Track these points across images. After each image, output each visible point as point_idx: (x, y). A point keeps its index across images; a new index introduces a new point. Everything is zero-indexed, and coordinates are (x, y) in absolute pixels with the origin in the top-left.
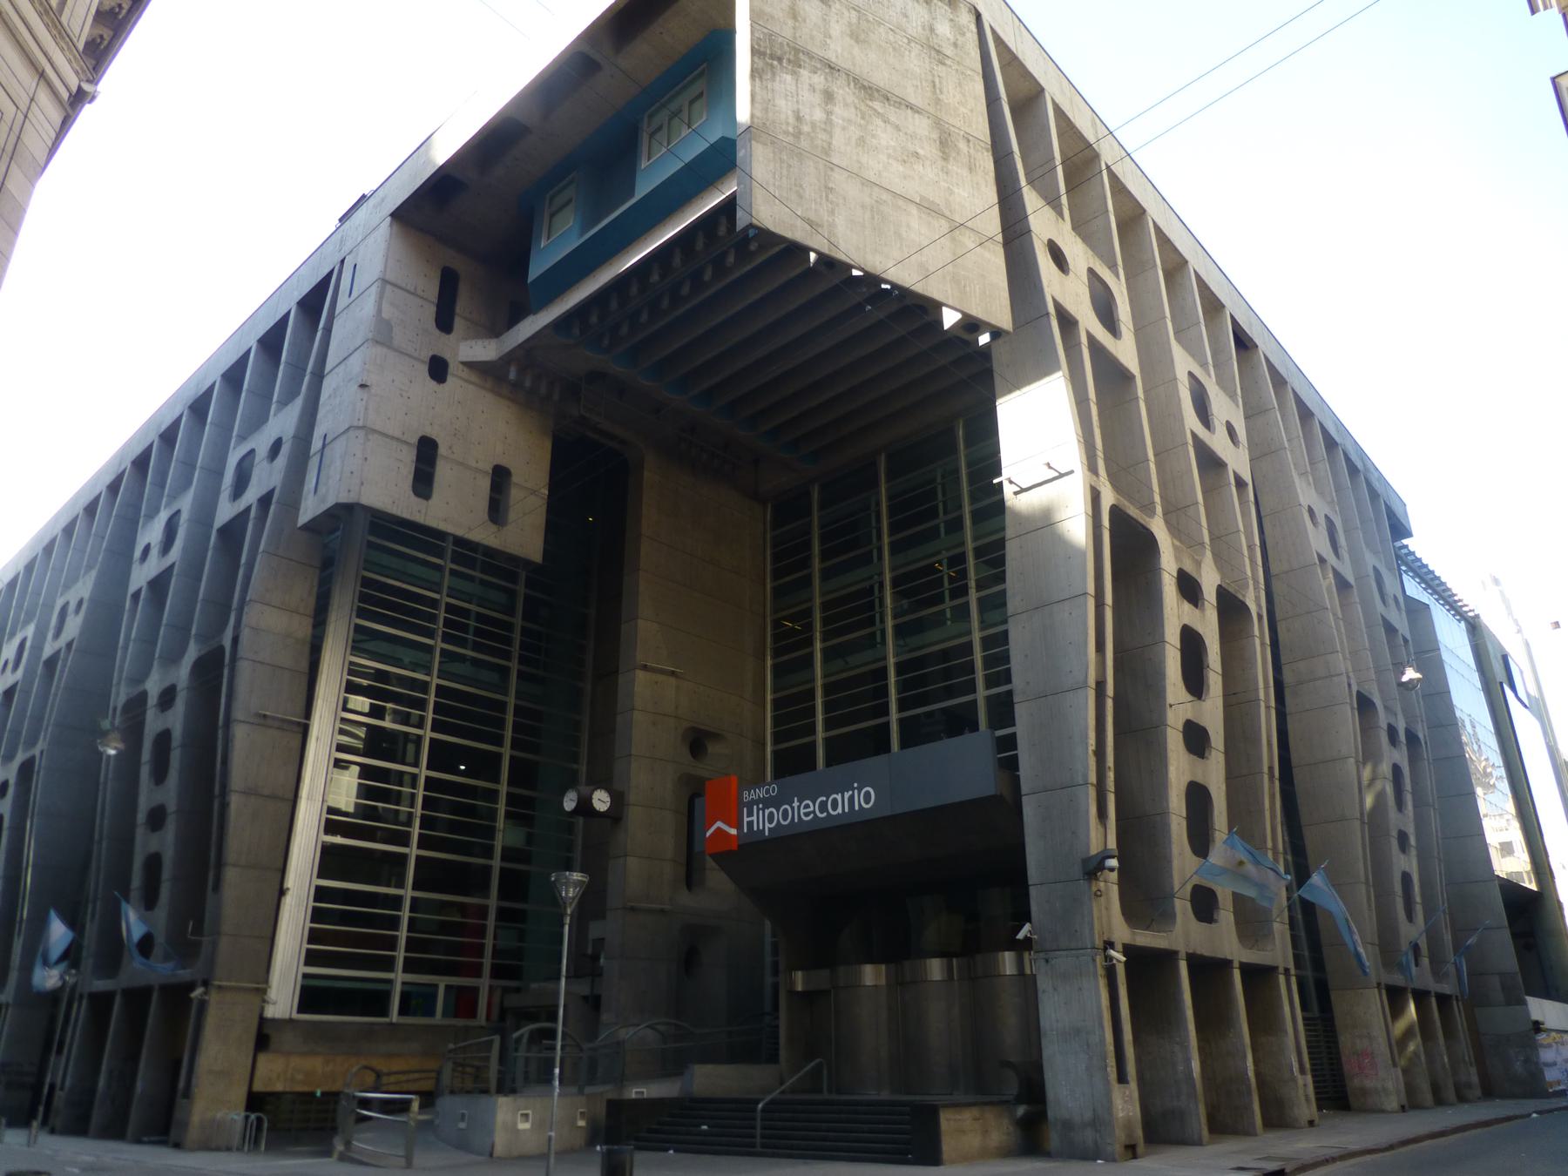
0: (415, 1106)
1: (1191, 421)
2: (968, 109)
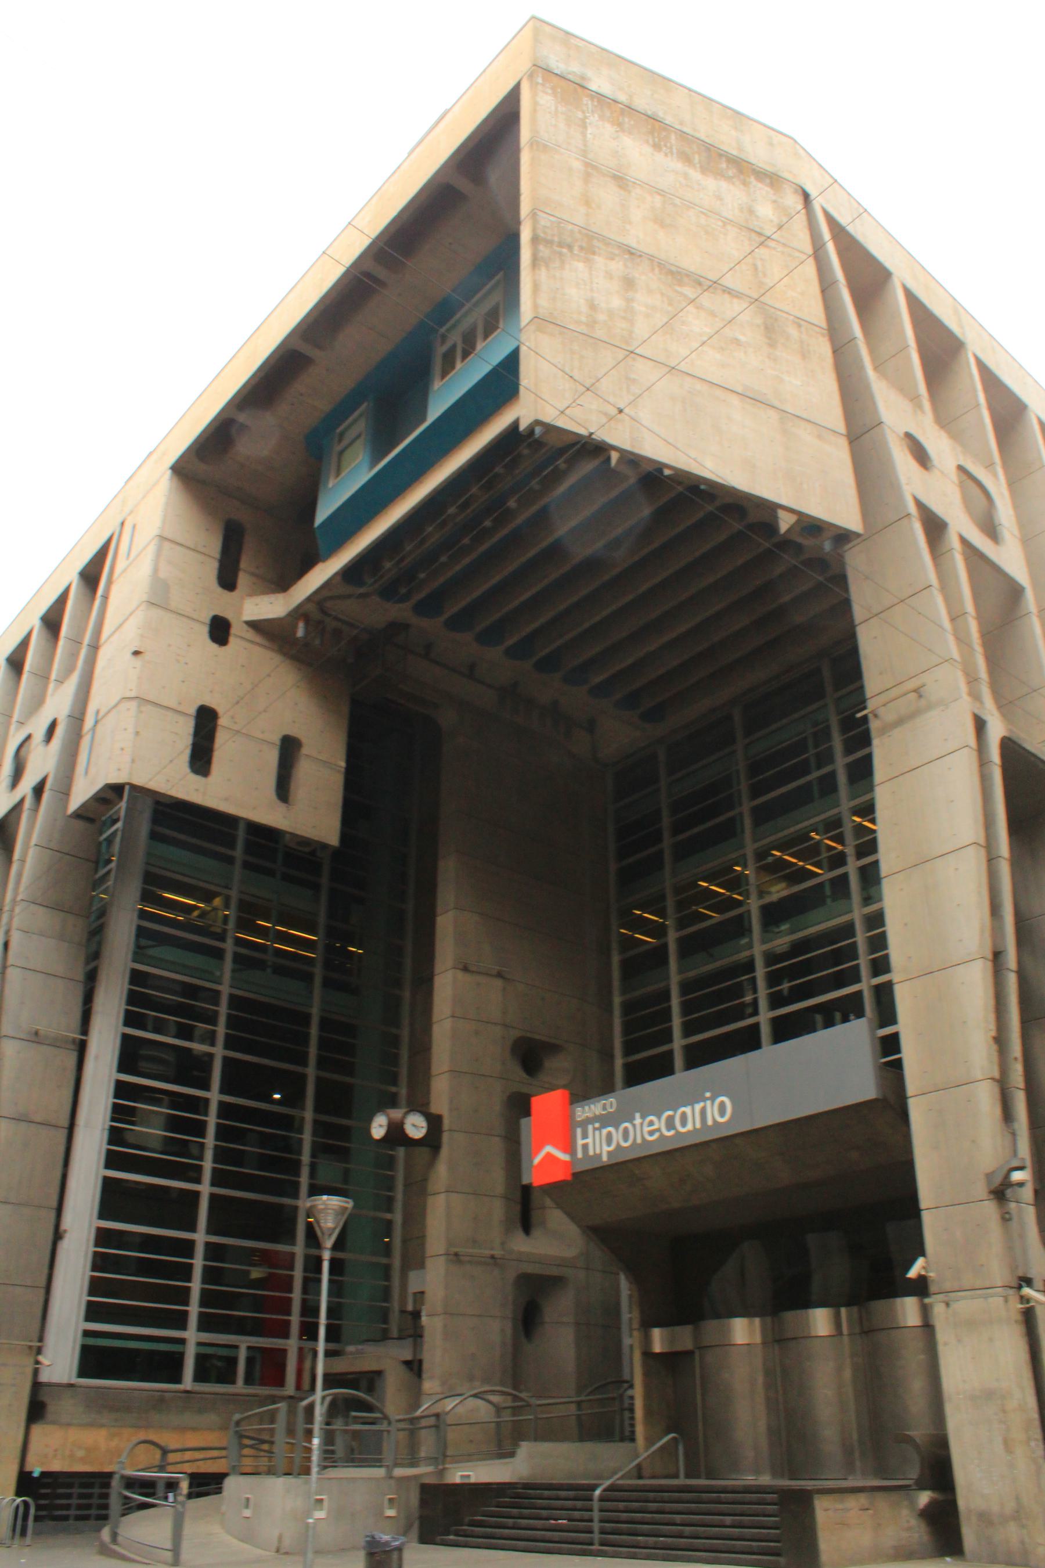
2: (799, 293)
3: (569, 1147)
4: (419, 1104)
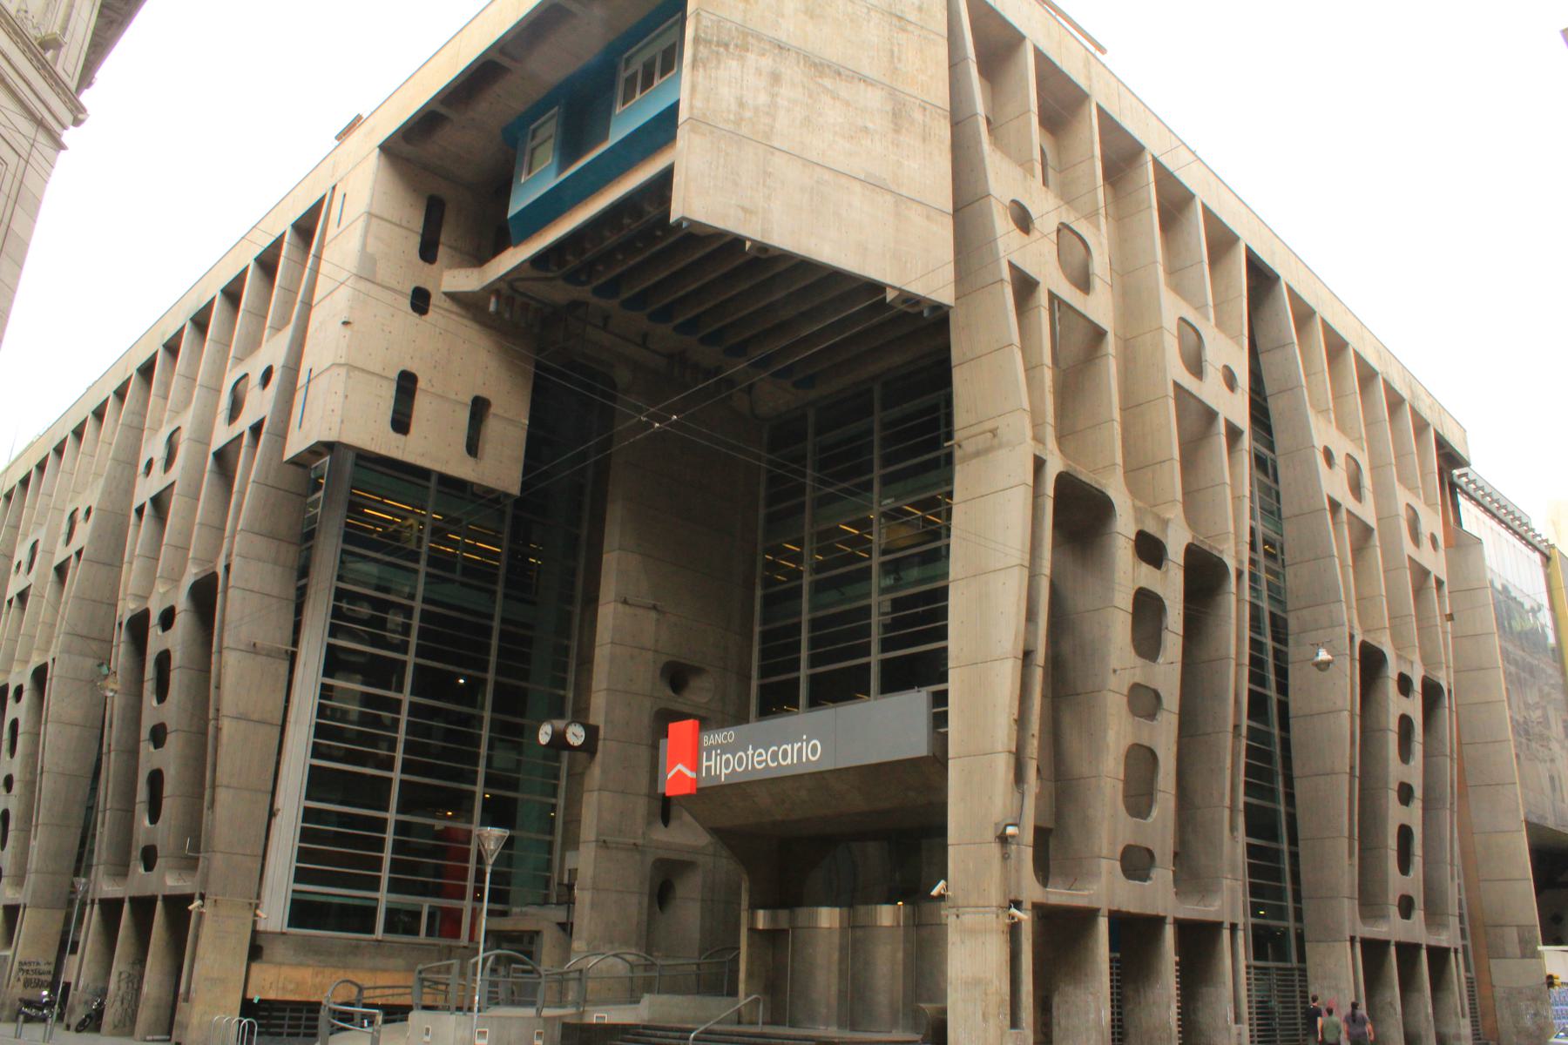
0: (380, 1018)
1: (1177, 371)
3: (696, 766)
4: (580, 716)
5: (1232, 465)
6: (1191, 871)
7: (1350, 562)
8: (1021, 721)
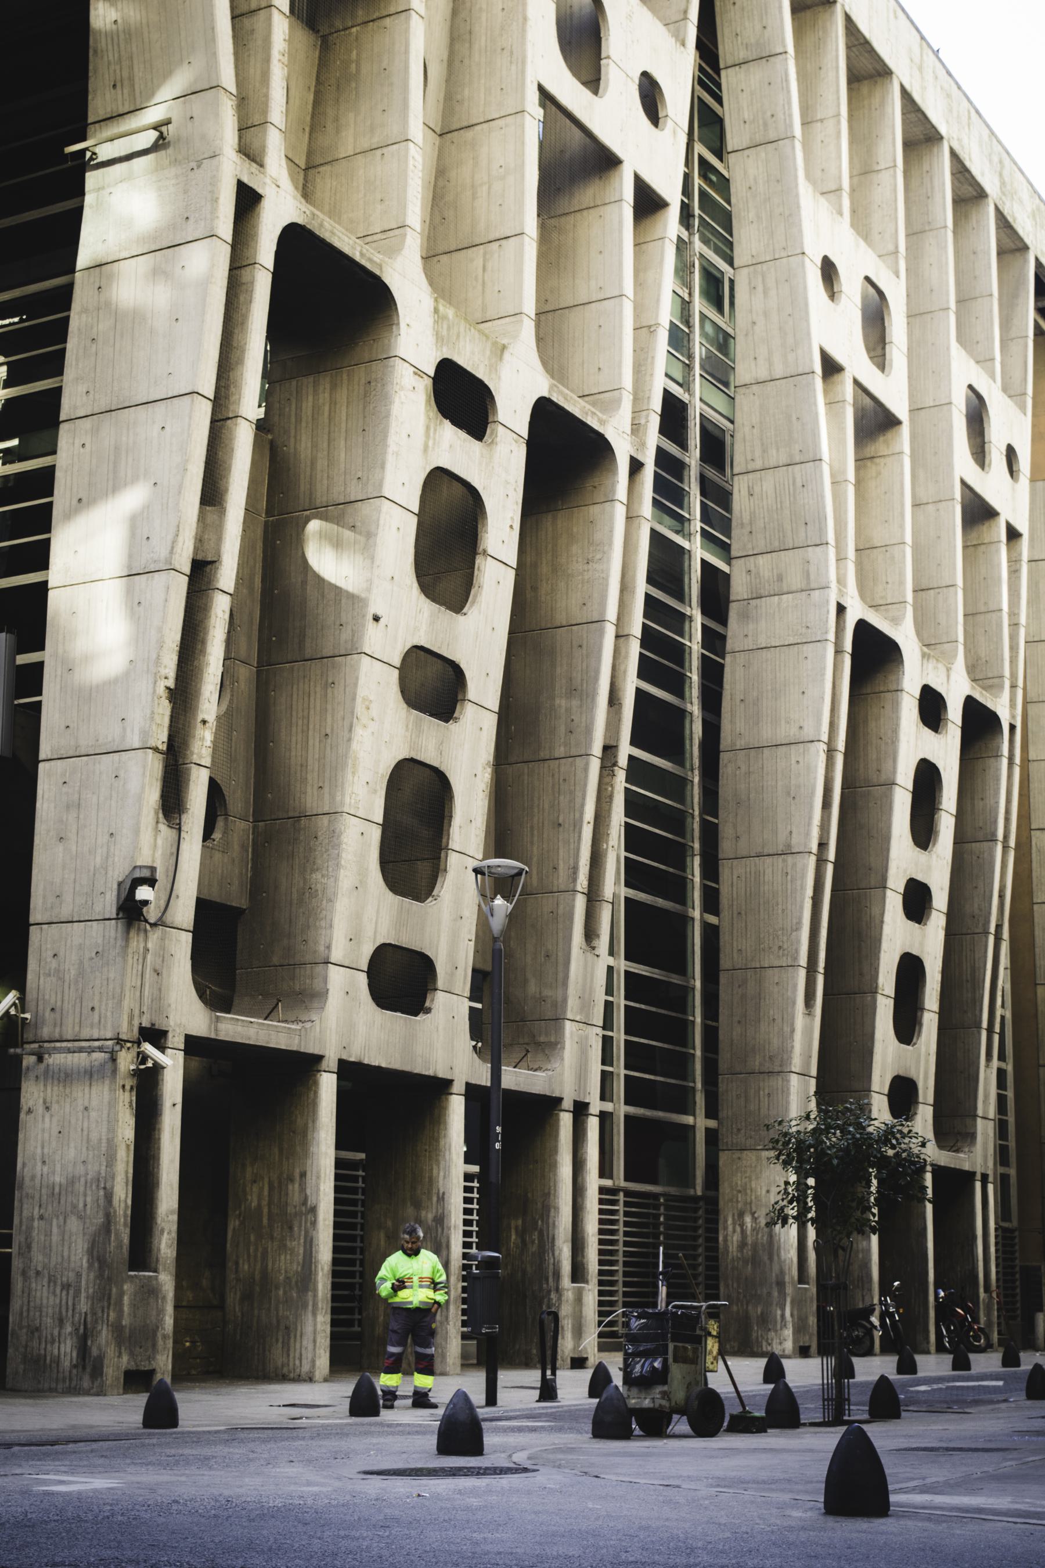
1: (546, 64)
5: (639, 269)
6: (509, 1006)
7: (851, 475)
8: (182, 695)
